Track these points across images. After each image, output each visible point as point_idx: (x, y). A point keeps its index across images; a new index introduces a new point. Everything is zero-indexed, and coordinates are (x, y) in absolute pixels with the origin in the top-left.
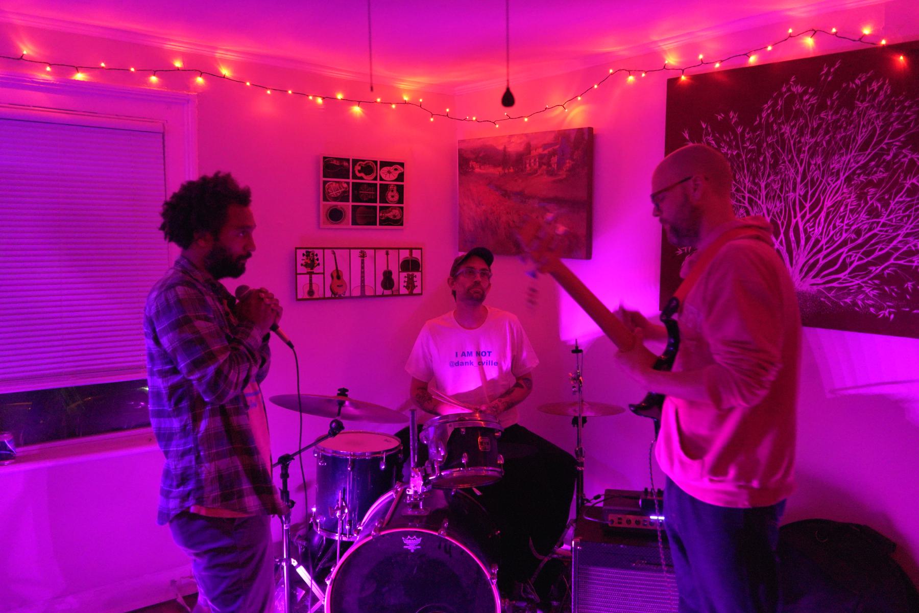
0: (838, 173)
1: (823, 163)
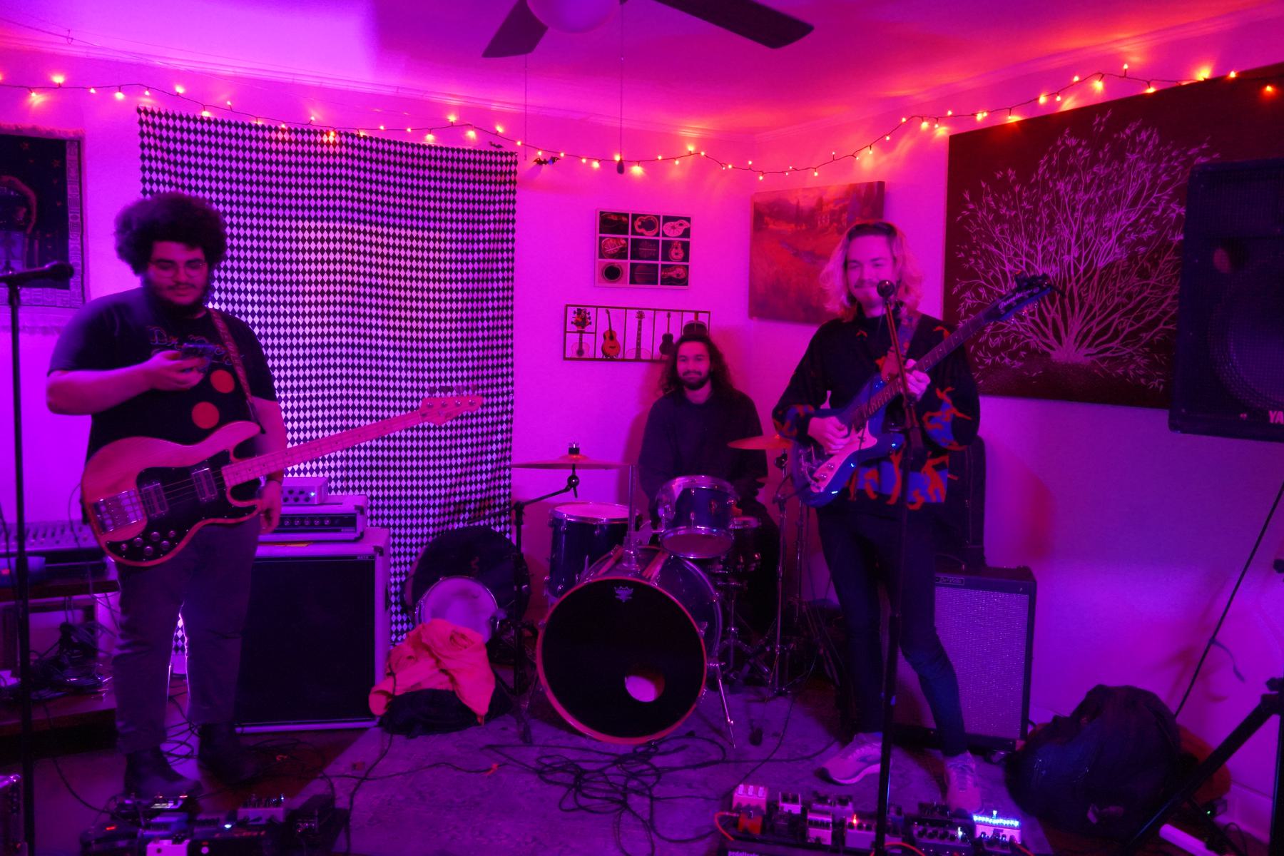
0: (1110, 231)
1: (1096, 222)
